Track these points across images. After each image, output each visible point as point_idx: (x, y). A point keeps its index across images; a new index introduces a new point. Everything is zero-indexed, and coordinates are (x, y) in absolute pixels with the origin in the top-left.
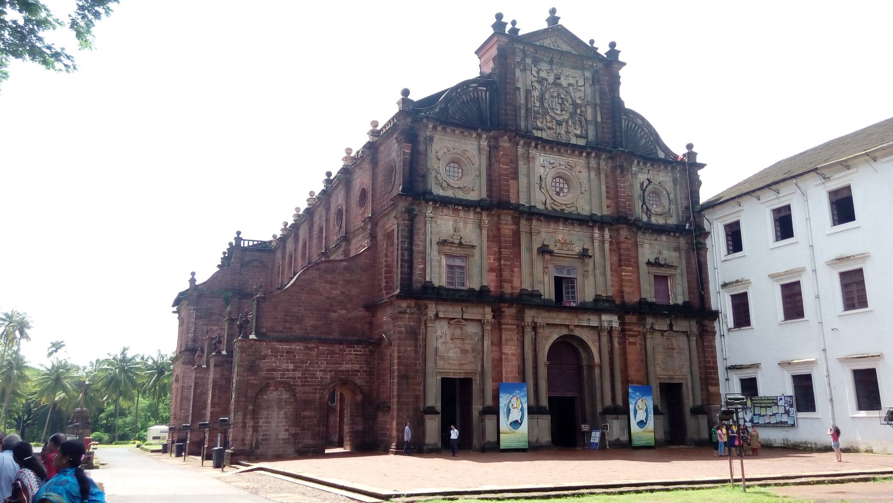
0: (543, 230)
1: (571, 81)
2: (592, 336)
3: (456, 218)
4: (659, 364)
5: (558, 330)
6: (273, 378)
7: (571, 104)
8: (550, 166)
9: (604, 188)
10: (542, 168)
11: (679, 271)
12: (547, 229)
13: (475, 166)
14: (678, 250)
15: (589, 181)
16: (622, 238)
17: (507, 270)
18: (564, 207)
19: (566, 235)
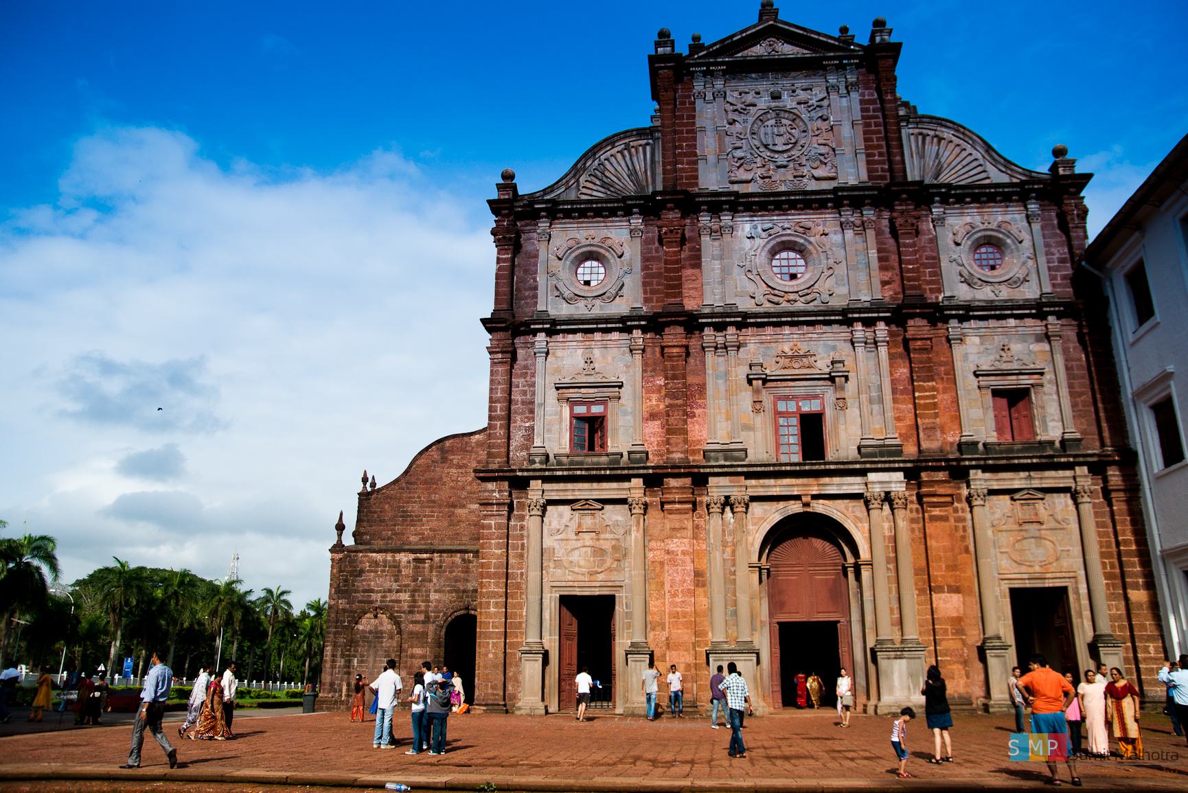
0: (753, 340)
1: (803, 96)
2: (853, 512)
3: (587, 343)
4: (1006, 552)
5: (782, 504)
6: (372, 602)
7: (804, 131)
8: (764, 235)
9: (873, 254)
10: (748, 244)
11: (1049, 376)
12: (758, 337)
13: (623, 258)
14: (1046, 341)
15: (844, 245)
16: (911, 332)
17: (676, 413)
18: (792, 297)
19: (799, 344)
